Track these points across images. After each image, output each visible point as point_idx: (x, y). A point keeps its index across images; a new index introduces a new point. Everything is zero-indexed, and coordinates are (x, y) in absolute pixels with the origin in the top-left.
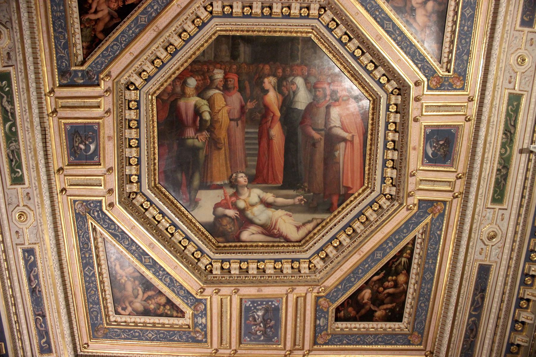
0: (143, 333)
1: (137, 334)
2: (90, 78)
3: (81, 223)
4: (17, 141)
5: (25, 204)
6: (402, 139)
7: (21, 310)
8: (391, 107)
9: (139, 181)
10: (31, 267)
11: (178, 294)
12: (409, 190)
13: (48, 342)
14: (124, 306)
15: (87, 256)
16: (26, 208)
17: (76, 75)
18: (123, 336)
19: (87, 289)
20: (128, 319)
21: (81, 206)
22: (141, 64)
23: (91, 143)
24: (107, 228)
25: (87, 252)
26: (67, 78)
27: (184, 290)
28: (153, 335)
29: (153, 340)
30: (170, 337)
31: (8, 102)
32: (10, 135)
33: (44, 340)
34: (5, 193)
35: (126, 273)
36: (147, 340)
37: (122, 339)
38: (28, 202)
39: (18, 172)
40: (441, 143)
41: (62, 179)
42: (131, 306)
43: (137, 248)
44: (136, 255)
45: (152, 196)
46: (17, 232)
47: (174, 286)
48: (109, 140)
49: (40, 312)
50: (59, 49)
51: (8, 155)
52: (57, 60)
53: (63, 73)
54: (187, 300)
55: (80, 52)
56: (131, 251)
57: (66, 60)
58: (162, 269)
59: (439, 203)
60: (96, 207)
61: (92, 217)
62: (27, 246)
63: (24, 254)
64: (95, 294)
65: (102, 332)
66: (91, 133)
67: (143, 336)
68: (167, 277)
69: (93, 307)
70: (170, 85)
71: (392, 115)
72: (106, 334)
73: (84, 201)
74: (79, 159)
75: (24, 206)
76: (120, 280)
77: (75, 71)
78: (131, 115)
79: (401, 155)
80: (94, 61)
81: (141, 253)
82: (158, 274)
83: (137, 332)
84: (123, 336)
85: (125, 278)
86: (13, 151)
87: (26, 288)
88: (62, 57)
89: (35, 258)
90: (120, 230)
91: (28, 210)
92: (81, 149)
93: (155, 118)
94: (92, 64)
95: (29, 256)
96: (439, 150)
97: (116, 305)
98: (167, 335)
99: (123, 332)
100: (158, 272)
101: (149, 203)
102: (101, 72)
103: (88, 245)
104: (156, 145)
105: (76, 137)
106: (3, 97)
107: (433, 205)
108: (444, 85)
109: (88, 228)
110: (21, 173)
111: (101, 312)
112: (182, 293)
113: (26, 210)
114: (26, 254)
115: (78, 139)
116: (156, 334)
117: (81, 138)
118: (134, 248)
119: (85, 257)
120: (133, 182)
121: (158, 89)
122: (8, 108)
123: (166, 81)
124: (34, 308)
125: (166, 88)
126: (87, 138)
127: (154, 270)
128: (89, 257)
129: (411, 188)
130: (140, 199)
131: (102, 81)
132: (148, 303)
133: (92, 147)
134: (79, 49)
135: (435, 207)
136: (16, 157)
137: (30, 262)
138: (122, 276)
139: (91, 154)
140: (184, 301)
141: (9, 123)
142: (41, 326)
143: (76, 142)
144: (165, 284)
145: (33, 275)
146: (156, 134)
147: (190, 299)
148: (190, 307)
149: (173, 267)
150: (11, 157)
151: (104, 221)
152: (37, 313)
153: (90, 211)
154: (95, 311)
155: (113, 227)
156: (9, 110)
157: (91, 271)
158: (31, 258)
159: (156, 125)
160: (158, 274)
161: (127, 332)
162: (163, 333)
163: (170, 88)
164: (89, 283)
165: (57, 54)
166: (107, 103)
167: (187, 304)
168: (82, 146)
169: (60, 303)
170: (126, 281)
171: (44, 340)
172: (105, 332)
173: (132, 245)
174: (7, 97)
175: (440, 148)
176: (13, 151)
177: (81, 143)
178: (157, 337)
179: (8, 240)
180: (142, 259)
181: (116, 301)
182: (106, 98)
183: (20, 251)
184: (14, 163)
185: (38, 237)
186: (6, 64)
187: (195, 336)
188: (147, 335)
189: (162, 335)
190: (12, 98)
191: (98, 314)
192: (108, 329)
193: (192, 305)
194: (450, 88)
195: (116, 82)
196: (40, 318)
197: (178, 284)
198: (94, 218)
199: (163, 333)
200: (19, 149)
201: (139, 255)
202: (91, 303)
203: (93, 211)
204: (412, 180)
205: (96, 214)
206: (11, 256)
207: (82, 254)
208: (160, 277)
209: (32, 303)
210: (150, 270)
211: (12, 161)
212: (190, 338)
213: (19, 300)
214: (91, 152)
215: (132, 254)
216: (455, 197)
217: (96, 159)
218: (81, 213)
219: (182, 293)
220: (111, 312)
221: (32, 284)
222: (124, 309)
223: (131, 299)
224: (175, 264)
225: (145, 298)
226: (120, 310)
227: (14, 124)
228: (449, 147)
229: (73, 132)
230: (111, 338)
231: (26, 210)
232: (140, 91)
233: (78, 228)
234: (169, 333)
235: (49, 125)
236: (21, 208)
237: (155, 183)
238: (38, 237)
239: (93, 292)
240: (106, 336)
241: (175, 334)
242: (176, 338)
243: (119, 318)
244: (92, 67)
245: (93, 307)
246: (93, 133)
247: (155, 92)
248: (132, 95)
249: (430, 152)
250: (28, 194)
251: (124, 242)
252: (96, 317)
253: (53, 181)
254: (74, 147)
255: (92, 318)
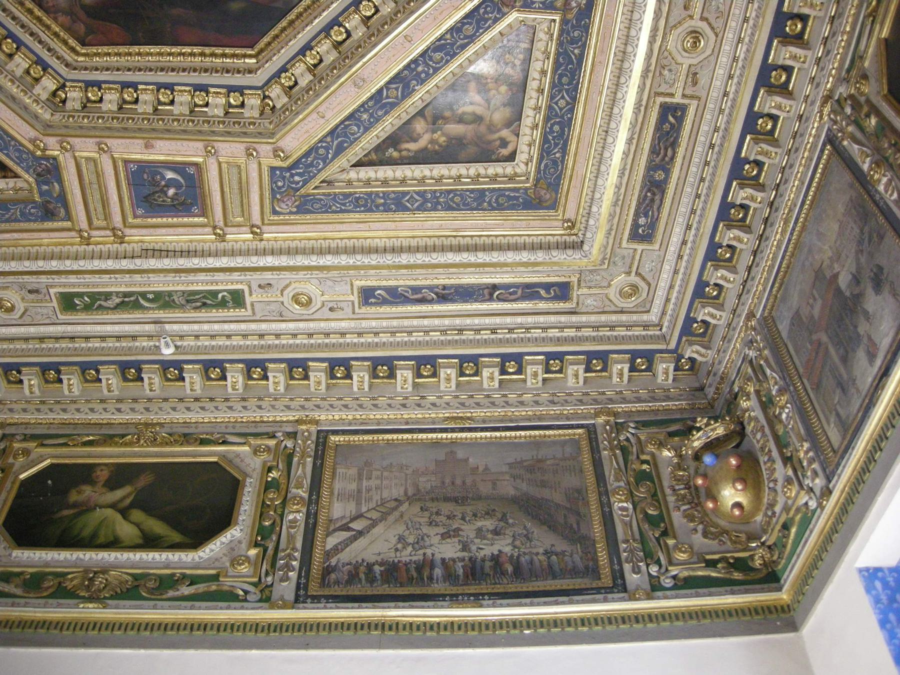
0: (556, 115)
1: (556, 128)
2: (49, 171)
3: (317, 206)
4: (170, 294)
5: (279, 293)
7: (477, 321)
9: (240, 90)
10: (395, 296)
11: (472, 39)
13: (547, 286)
14: (498, 143)
15: (382, 201)
16: (285, 293)
17: (49, 193)
18: (557, 155)
19: (450, 208)
20: (525, 139)
21: (283, 202)
22: (11, 80)
23: (163, 178)
24: (324, 162)
25: (373, 201)
26: (55, 208)
27: (464, 24)
28: (563, 97)
29: (574, 99)
30: (572, 63)
31: (106, 300)
32: (161, 302)
33: (543, 292)
34: (263, 318)
35: (427, 131)
36: (572, 110)
37: (563, 157)
38: (275, 288)
39: (223, 297)
41: (234, 230)
42: (499, 130)
43: (366, 111)
44: (380, 113)
45: (271, 68)
46: (331, 309)
47: (452, 45)
48: (152, 146)
49: (486, 291)
50: (10, 218)
51: (196, 308)
52: (30, 221)
53: (48, 214)
54: (486, 20)
55: (11, 182)
56: (371, 123)
57: (25, 208)
58: (413, 66)
60: (284, 178)
61: (302, 187)
62: (355, 298)
63: (372, 304)
64: (460, 195)
65: (543, 192)
66: (145, 176)
67: (562, 117)
68: (431, 59)
69: (489, 203)
70: (55, 19)
72: (549, 185)
73: (274, 197)
74: (195, 198)
75: (282, 295)
76: (440, 146)
77: (41, 194)
78: (111, 100)
80: (18, 164)
81: (375, 104)
82: (423, 75)
83: (551, 128)
84: (557, 155)
85: (436, 136)
86: (188, 301)
87: (438, 308)
88: (23, 214)
89: (379, 288)
90: (329, 139)
91: (289, 289)
92: (176, 194)
93: (123, 49)
94: (23, 168)
95: (375, 297)
97: (493, 157)
98: (566, 69)
99: (548, 153)
100: (419, 74)
101: (283, 75)
102: (33, 154)
103: (360, 198)
104: (174, 50)
105: (155, 200)
106: (100, 305)
109: (324, 194)
110: (225, 293)
111: (499, 189)
112: (469, 29)
113: (289, 293)
114: (373, 300)
115: (159, 197)
116: (560, 91)
117: (157, 192)
118: (365, 116)
119: (383, 205)
120: (243, 102)
121: (65, 43)
122: (118, 300)
123: (48, 27)
124: (476, 301)
125: (62, 26)
126: (155, 183)
127: (414, 82)
128: (383, 198)
130: (275, 91)
131: (48, 153)
132: (494, 95)
133: (170, 175)
134: (7, 184)
136: (197, 297)
137: (388, 297)
138: (432, 141)
139: (183, 179)
140: (489, 27)
141: (142, 302)
142: (515, 293)
143: (164, 201)
144: (447, 62)
145: (413, 294)
146: (154, 49)
147: (486, 12)
148: (504, 14)
149: (407, 44)
150: (199, 304)
151: (311, 165)
152: (487, 297)
153: (292, 188)
154: (497, 199)
155: (322, 151)
156: (121, 300)
157: (412, 197)
158: (379, 294)
159: (136, 49)
160: (423, 75)
161: (549, 147)
162: (561, 76)
163: (61, 18)
164: (438, 203)
165: (20, 221)
166: (86, 148)
167: (496, 20)
168: (171, 192)
169: (465, 261)
170: (443, 134)
171: (543, 292)
172: (545, 186)
173: (359, 120)
174: (100, 300)
176: (188, 301)
177: (166, 194)
178: (567, 91)
179: (344, 325)
180: (388, 103)
181: (486, 156)
182: (77, 148)
183: (364, 310)
184: (209, 302)
185: (339, 279)
186: (47, 297)
187: (575, 11)
188: (561, 109)
189: (565, 80)
190: (99, 293)
191: (504, 195)
192: (537, 180)
193: (499, 11)
195: (48, 128)
196: (497, 293)
197: (448, 36)
198: (305, 183)
199: (561, 76)
200: (184, 292)
201: (381, 108)
202: (479, 205)
203: (292, 183)
205: (297, 178)
206: (374, 323)
207: (378, 211)
208: (431, 71)
209: (467, 302)
210: (414, 90)
211: (204, 304)
212: (579, 20)
213: (458, 321)
214: (179, 178)
215: (377, 120)
217: (192, 170)
218: (297, 203)
219: (469, 29)
220: (509, 169)
221: (429, 298)
222: (504, 143)
223: (483, 129)
224: (401, 39)
225: (482, 102)
226: (505, 152)
227: (143, 295)
229: (147, 205)
230: (559, 178)
231: (289, 293)
232: (66, 80)
233: (326, 212)
234: (561, 65)
235: (137, 242)
236: (287, 298)
237: (251, 56)
238: (339, 279)
239: (457, 199)
240: (555, 186)
241: (566, 51)
242: (576, 51)
243: (521, 157)
244: (30, 167)
245: (489, 203)
246: (144, 172)
247: (73, 50)
248: (74, 96)
250: (260, 286)
251: (353, 134)
252: (510, 198)
253: (237, 246)
254: (174, 206)
255: (513, 207)
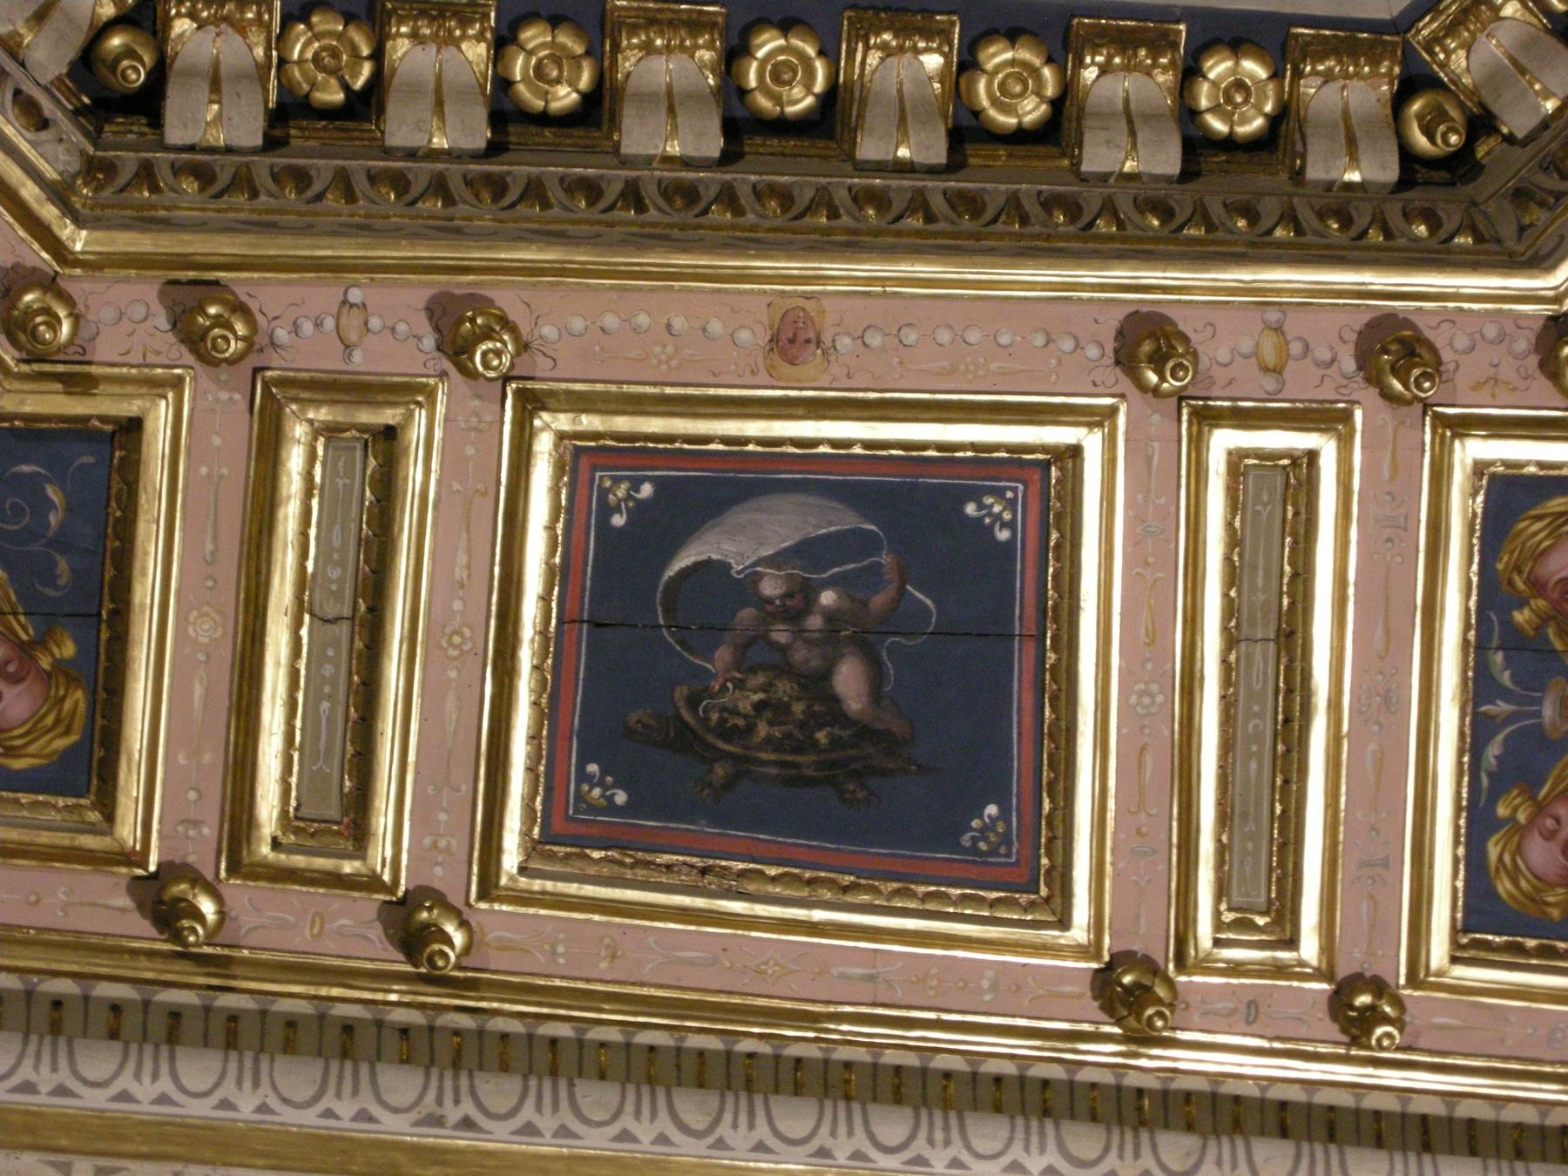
6: (879, 199)
8: (1253, 68)
12: (271, 296)
40: (849, 681)
59: (77, 699)
71: (1156, 82)
79: (689, 194)
96: (755, 655)
107: (48, 619)
108: (1531, 686)
129: (301, 317)
135: (27, 650)
175: (782, 666)
194: (1493, 750)
204: (389, 326)
216: (161, 901)
228: (796, 780)
249: (735, 543)
